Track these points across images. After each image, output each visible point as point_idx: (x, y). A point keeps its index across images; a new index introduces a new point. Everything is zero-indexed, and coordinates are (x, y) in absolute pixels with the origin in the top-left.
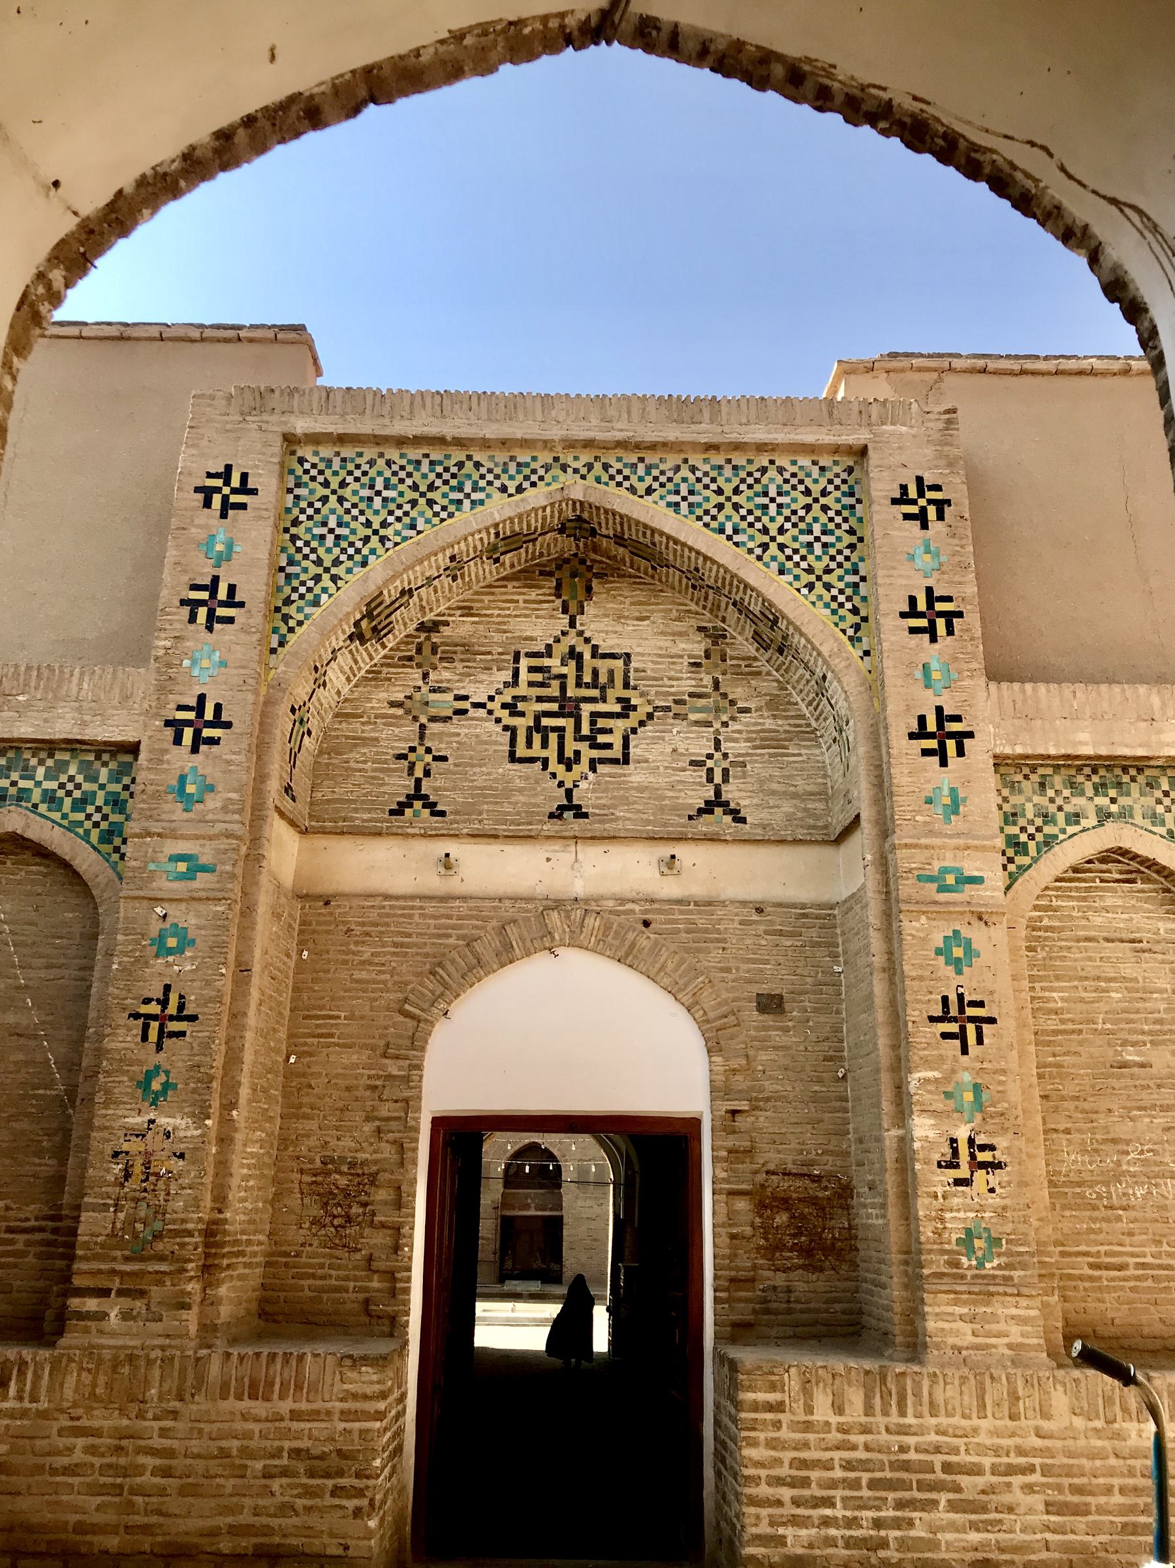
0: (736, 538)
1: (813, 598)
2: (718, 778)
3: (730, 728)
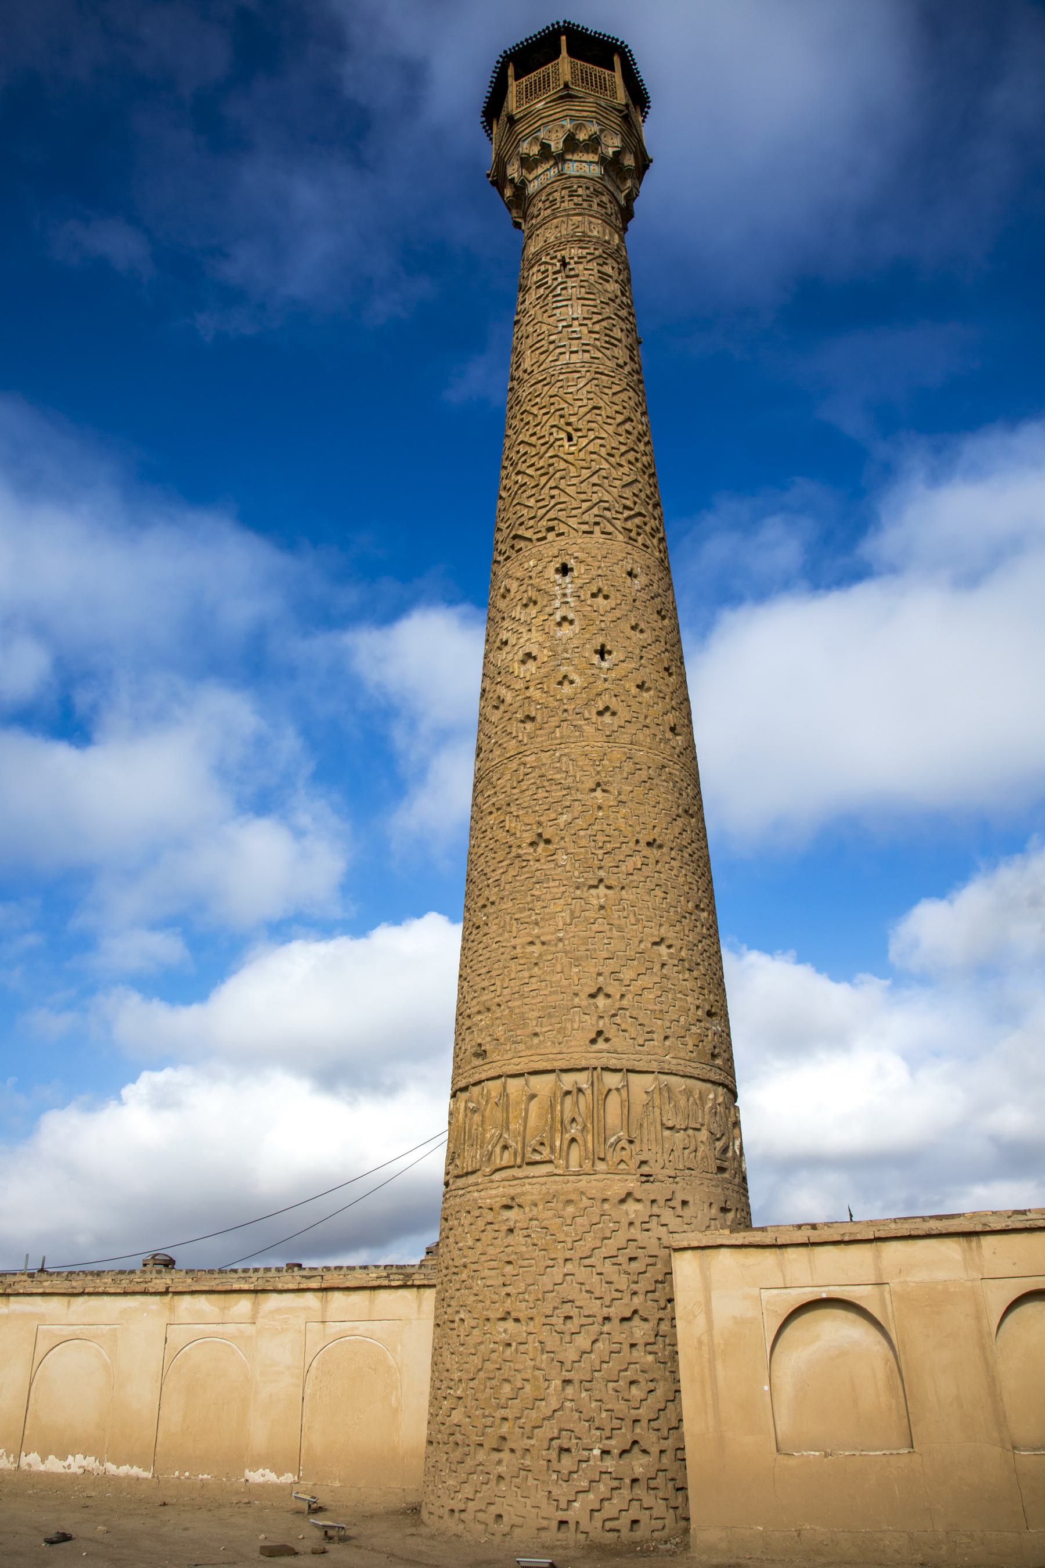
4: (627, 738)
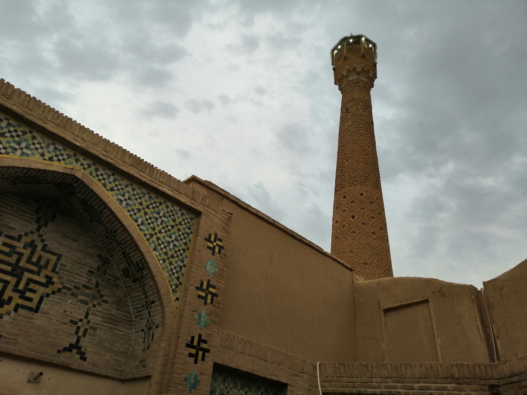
0: (141, 227)
1: (164, 266)
2: (81, 333)
3: (96, 309)
4: (358, 238)
